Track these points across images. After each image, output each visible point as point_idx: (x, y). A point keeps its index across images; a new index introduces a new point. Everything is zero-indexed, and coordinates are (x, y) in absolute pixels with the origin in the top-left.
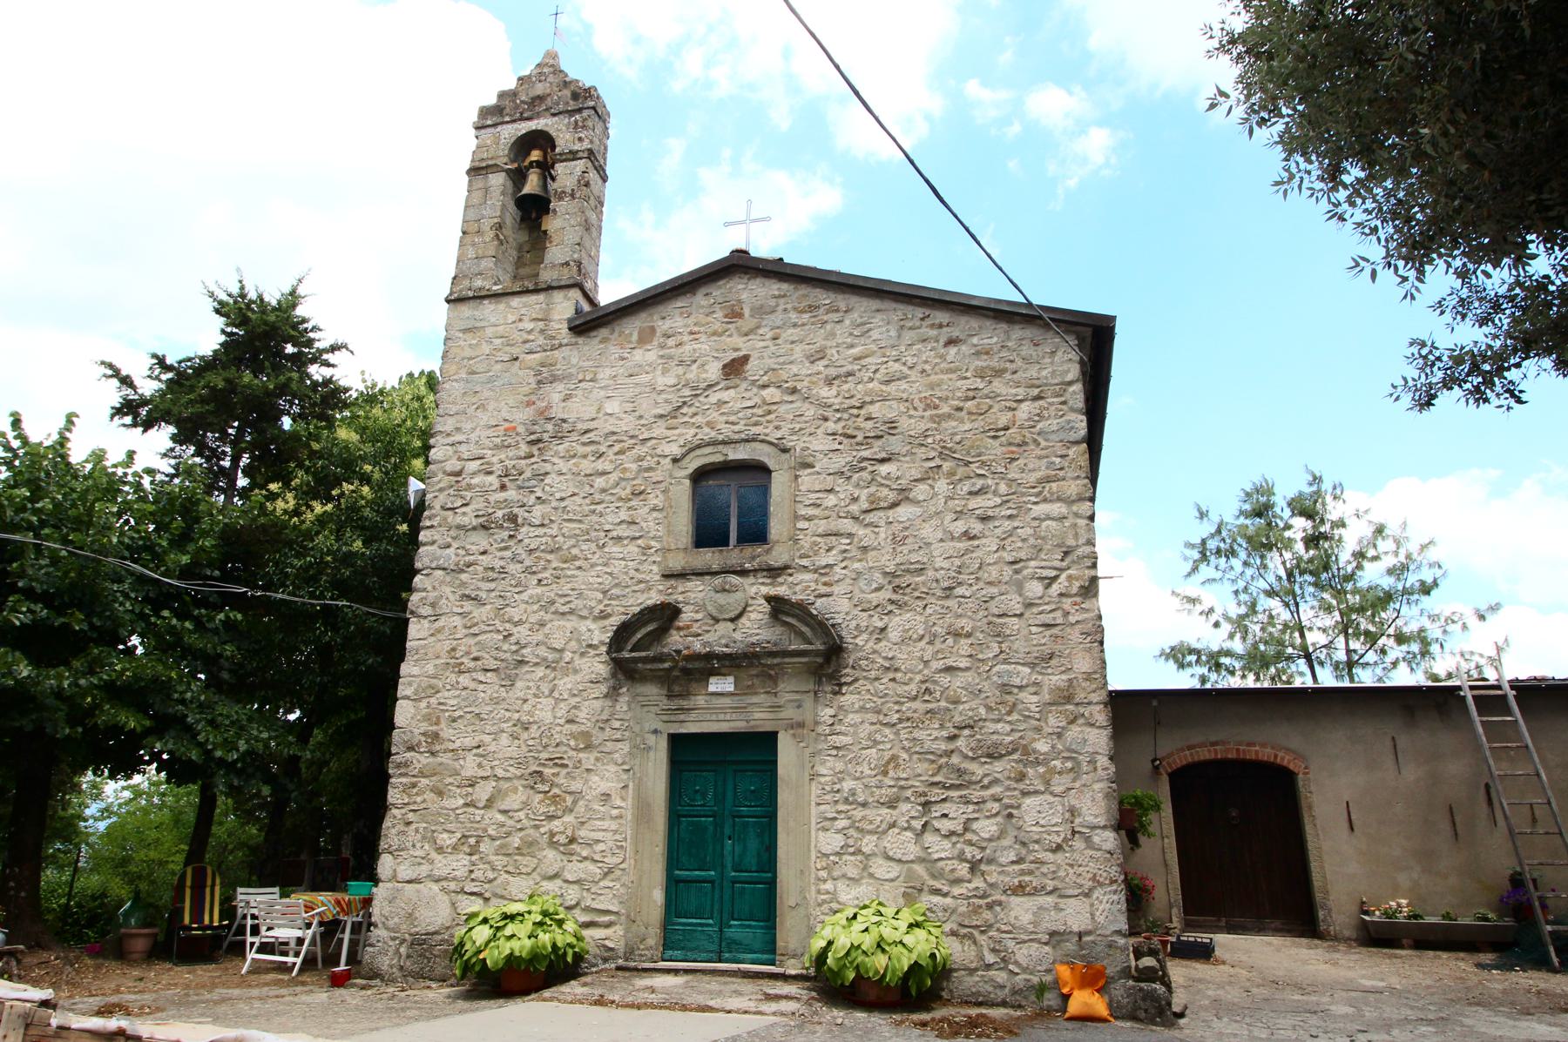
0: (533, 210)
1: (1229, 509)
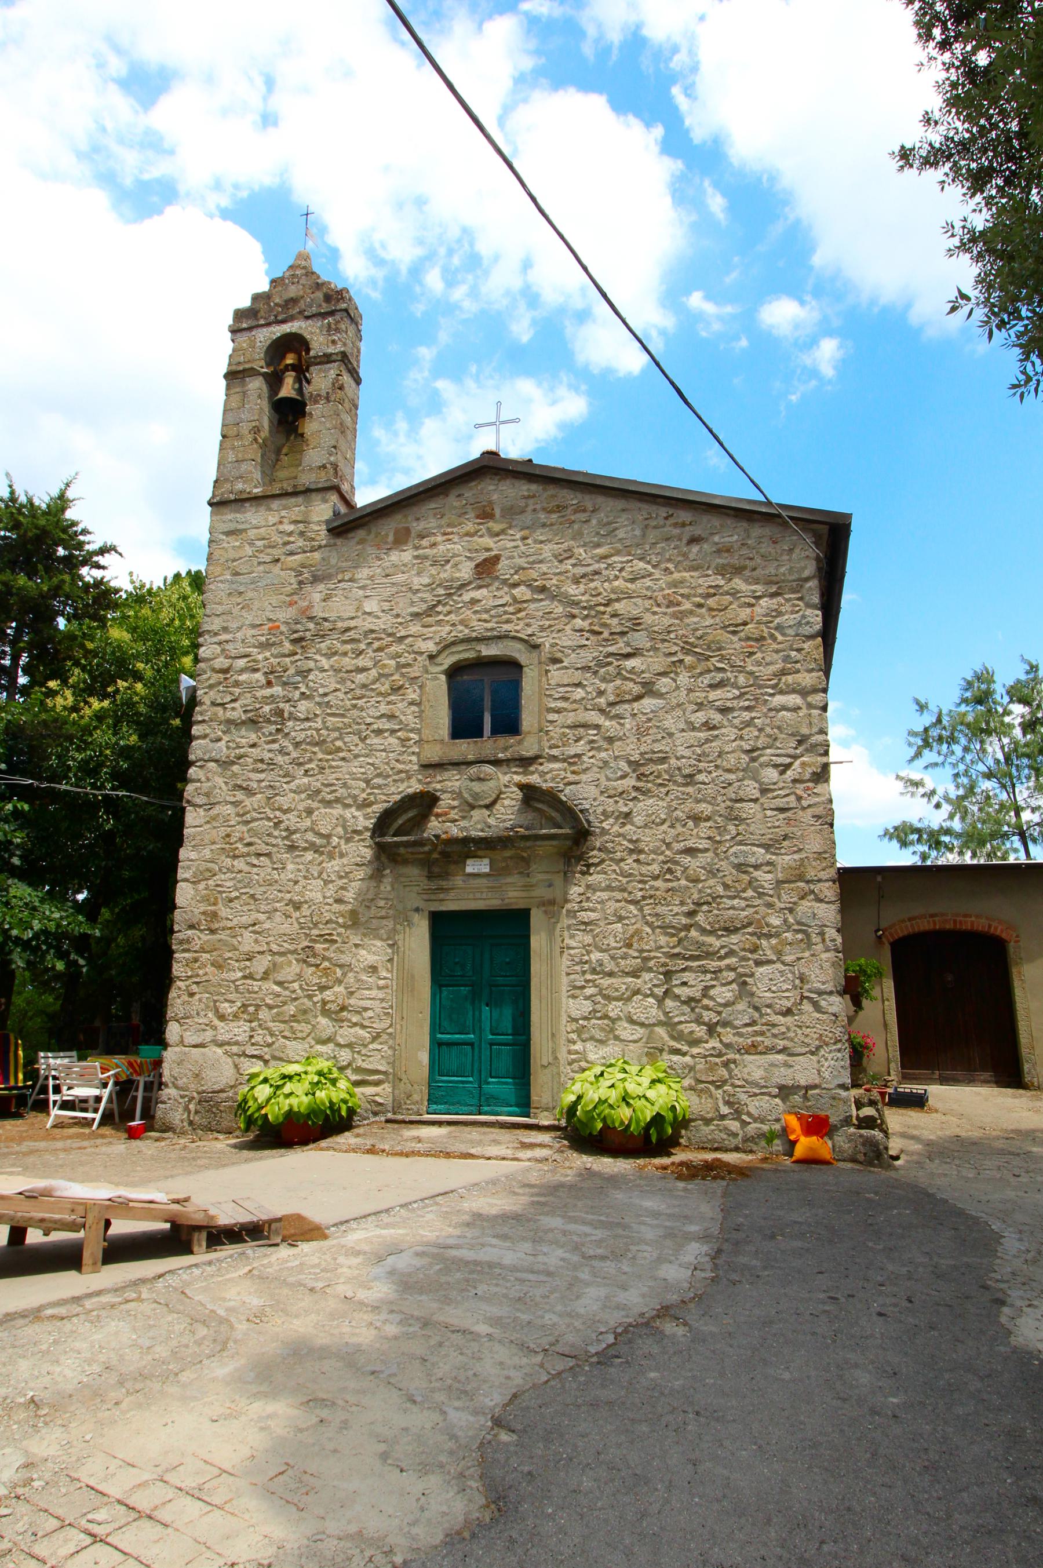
0: (289, 415)
1: (947, 698)
